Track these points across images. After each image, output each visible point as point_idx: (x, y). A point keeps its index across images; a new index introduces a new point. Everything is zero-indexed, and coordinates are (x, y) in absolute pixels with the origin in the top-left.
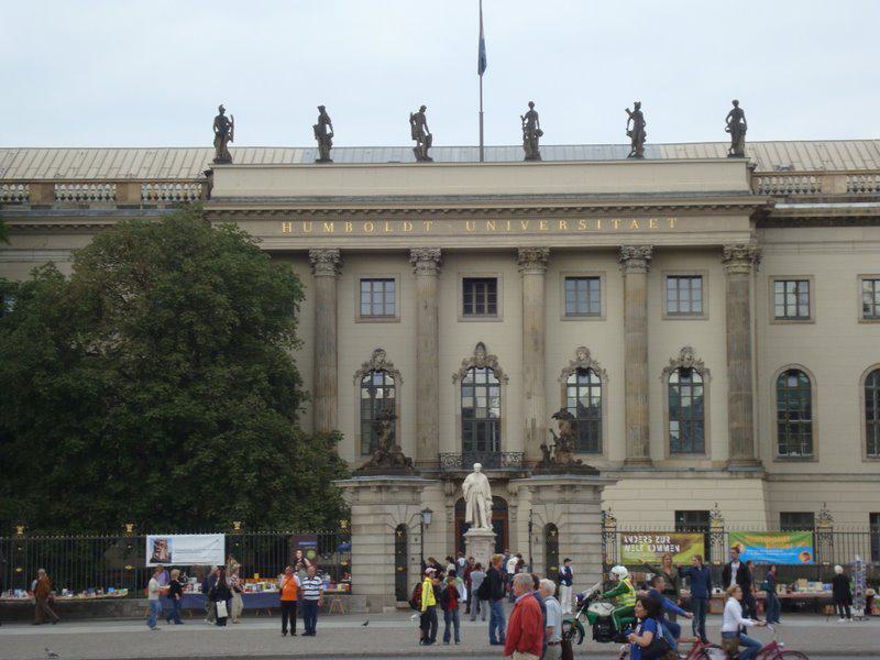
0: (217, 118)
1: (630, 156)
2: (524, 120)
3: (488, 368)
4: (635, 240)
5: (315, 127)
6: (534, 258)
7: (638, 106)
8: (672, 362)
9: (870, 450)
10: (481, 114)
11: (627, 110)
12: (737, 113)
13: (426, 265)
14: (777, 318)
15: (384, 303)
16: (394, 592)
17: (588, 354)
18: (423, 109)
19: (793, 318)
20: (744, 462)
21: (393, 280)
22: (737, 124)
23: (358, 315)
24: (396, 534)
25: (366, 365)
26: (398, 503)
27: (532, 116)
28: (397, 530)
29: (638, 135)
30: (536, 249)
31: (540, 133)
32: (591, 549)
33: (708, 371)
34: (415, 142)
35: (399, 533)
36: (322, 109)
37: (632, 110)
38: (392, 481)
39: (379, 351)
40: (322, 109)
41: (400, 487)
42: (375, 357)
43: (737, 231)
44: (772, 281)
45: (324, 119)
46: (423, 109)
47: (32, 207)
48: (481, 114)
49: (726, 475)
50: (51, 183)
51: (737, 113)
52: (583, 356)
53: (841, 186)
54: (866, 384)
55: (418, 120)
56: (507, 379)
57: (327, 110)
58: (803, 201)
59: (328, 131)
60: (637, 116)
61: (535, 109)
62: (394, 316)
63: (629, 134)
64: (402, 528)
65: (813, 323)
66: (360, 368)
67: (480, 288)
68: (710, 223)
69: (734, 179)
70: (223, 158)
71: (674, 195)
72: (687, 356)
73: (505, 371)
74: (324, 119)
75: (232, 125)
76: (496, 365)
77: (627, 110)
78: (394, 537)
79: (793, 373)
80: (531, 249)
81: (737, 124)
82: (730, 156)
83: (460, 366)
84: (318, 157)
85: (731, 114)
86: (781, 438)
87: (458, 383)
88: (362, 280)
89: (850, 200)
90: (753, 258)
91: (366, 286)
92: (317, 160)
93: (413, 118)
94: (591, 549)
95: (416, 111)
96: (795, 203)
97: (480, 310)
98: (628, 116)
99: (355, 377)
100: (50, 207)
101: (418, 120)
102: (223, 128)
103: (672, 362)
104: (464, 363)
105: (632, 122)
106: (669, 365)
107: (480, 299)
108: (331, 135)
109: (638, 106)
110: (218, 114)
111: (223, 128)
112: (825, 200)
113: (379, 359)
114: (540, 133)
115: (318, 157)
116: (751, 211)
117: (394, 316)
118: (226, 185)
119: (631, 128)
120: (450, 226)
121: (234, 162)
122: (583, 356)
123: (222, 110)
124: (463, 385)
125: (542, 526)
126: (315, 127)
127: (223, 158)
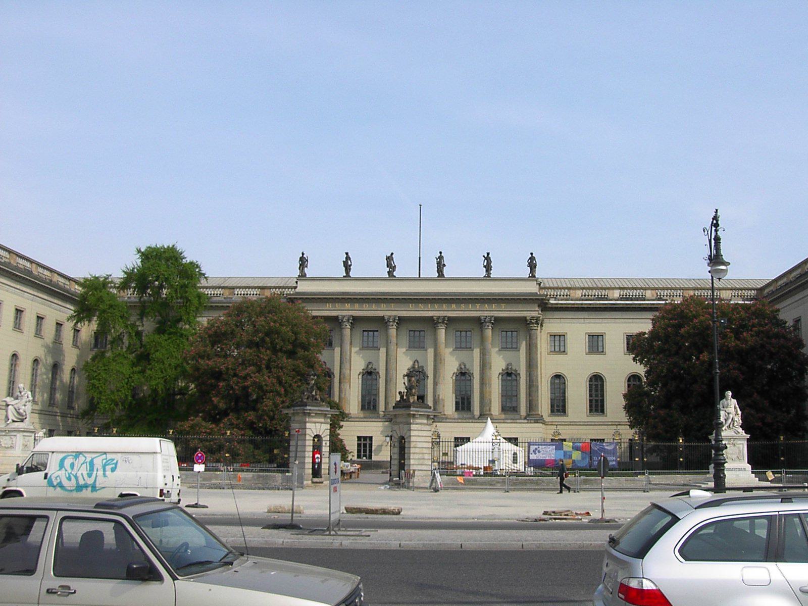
0: (300, 258)
1: (485, 276)
3: (420, 372)
4: (486, 314)
5: (344, 262)
7: (488, 254)
8: (503, 370)
9: (591, 411)
10: (420, 258)
11: (484, 256)
12: (532, 258)
14: (551, 352)
15: (373, 341)
16: (311, 473)
17: (465, 366)
18: (392, 254)
19: (557, 352)
20: (532, 415)
21: (377, 331)
22: (532, 264)
24: (314, 440)
25: (363, 370)
26: (315, 423)
27: (441, 258)
28: (314, 437)
29: (488, 268)
31: (444, 265)
32: (425, 451)
33: (519, 374)
34: (388, 269)
35: (316, 440)
36: (347, 254)
37: (486, 256)
38: (310, 410)
39: (370, 363)
40: (347, 254)
41: (316, 413)
42: (368, 366)
43: (532, 312)
44: (549, 336)
45: (348, 258)
46: (392, 254)
47: (225, 298)
48: (420, 258)
49: (526, 421)
50: (233, 288)
51: (532, 258)
52: (463, 367)
53: (579, 293)
54: (590, 381)
55: (390, 259)
57: (349, 254)
58: (562, 300)
59: (349, 263)
60: (487, 258)
62: (377, 347)
63: (485, 267)
64: (317, 436)
65: (567, 354)
68: (520, 307)
69: (531, 288)
70: (303, 276)
71: (503, 294)
72: (510, 367)
74: (348, 258)
75: (307, 261)
76: (423, 370)
77: (484, 256)
78: (312, 442)
79: (558, 376)
81: (532, 264)
82: (529, 277)
84: (345, 275)
85: (530, 258)
86: (552, 406)
88: (364, 331)
89: (583, 300)
90: (538, 322)
91: (366, 333)
92: (344, 276)
93: (388, 258)
94: (425, 451)
95: (389, 255)
96: (559, 300)
99: (359, 375)
100: (231, 298)
101: (390, 259)
102: (303, 262)
105: (486, 261)
106: (501, 371)
108: (350, 265)
109: (488, 254)
110: (301, 255)
111: (303, 262)
112: (572, 300)
113: (370, 366)
114: (444, 265)
115: (345, 275)
116: (539, 302)
117: (377, 347)
118: (304, 287)
119: (485, 264)
120: (402, 306)
121: (307, 276)
122: (463, 367)
123: (303, 254)
125: (397, 437)
126: (344, 262)
127: (303, 276)
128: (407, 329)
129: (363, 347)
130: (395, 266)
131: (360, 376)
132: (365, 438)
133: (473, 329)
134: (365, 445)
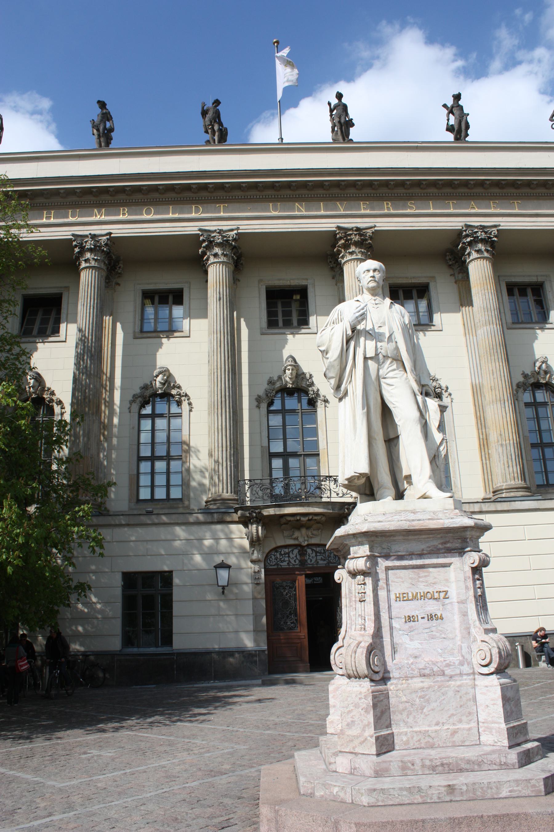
2: (331, 111)
6: (357, 238)
8: (525, 376)
11: (445, 106)
13: (217, 250)
18: (217, 103)
23: (138, 329)
30: (358, 229)
36: (102, 105)
37: (450, 103)
40: (102, 105)
46: (217, 103)
56: (326, 401)
61: (344, 100)
63: (450, 129)
66: (138, 391)
67: (287, 305)
73: (322, 393)
77: (445, 106)
80: (352, 229)
83: (265, 386)
87: (264, 406)
95: (209, 104)
97: (288, 324)
98: (446, 111)
99: (132, 402)
103: (525, 376)
104: (271, 382)
106: (521, 379)
107: (287, 314)
108: (112, 130)
109: (457, 97)
124: (269, 412)
128: (260, 281)
129: (142, 331)
130: (226, 129)
131: (135, 407)
132: (149, 577)
133: (433, 278)
134: (149, 601)
